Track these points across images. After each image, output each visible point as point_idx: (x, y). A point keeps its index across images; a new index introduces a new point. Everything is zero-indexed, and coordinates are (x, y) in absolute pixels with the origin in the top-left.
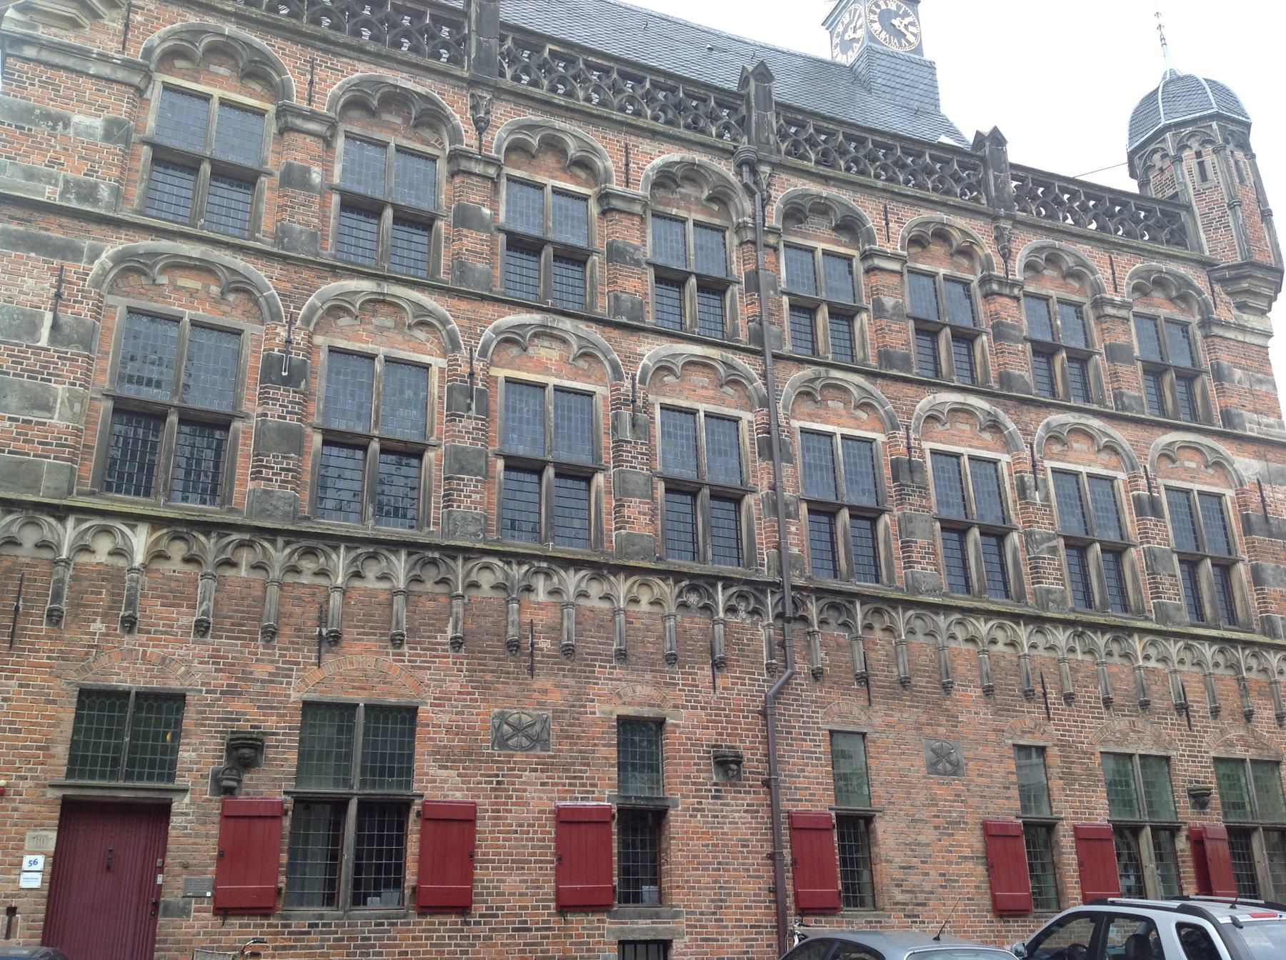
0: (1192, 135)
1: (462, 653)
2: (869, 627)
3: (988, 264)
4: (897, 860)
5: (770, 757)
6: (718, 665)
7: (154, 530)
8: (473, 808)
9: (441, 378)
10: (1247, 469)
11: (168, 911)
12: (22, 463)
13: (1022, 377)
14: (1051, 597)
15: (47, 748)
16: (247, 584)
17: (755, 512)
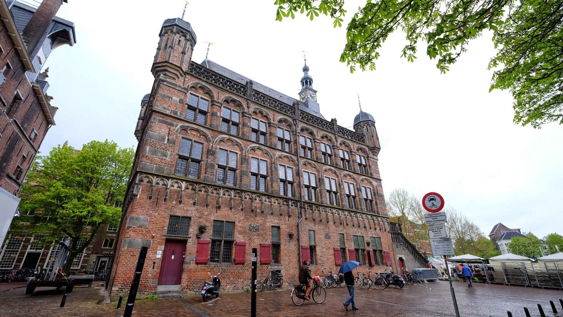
0: (366, 123)
1: (243, 212)
2: (315, 210)
3: (334, 143)
5: (298, 235)
6: (289, 216)
7: (186, 183)
8: (245, 243)
9: (240, 156)
11: (186, 264)
12: (160, 167)
15: (163, 228)
16: (203, 195)
17: (296, 187)
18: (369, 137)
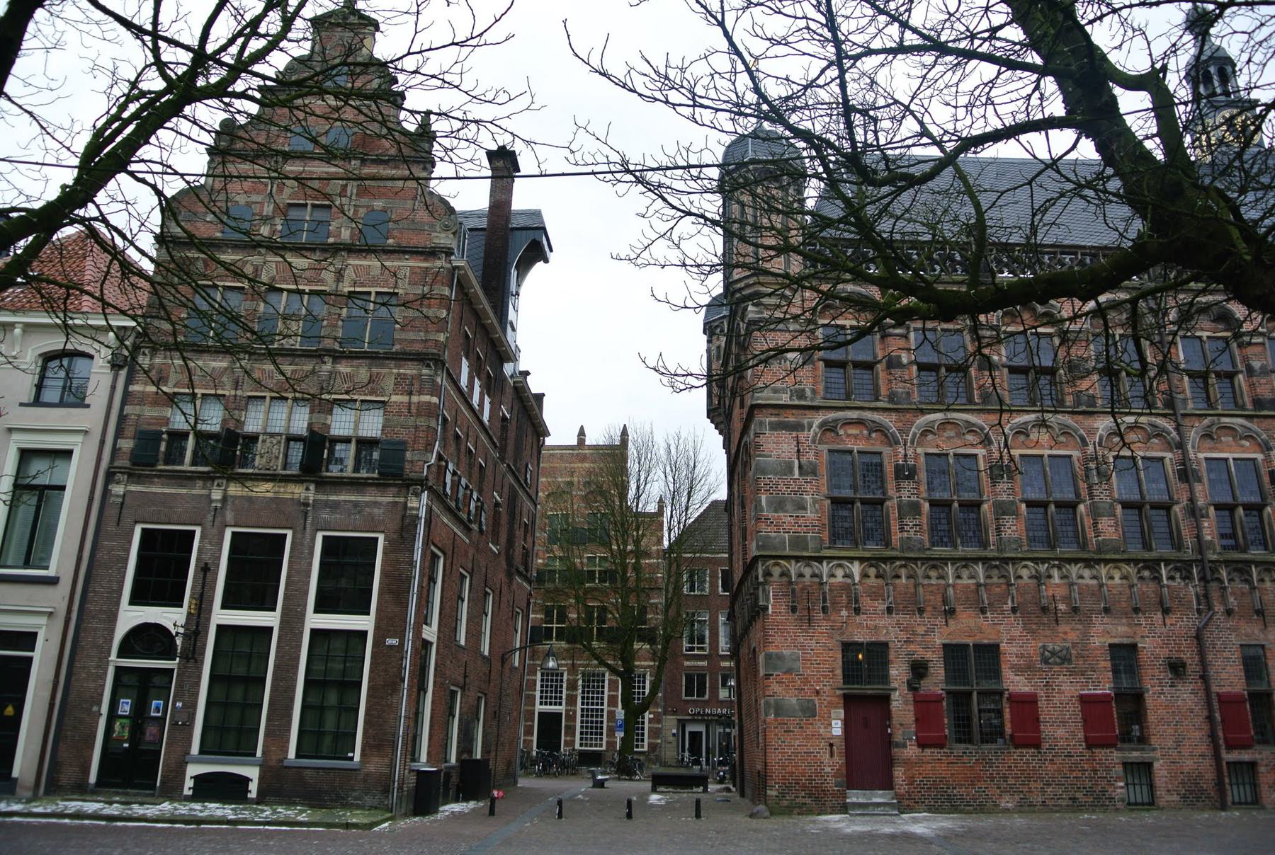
1: (1018, 615)
2: (1262, 580)
5: (1203, 663)
6: (1166, 611)
7: (861, 563)
8: (1035, 695)
9: (985, 461)
11: (897, 745)
12: (798, 537)
16: (906, 587)
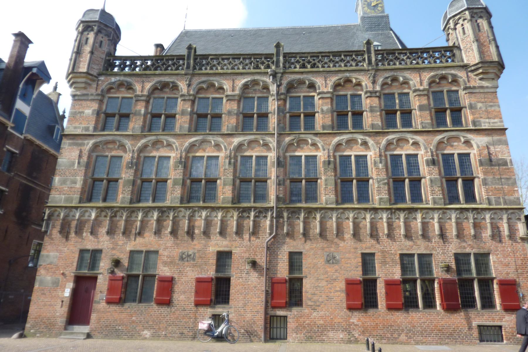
4: (310, 292)
10: (481, 142)
13: (377, 124)
14: (382, 200)
15: (72, 264)
18: (469, 46)
